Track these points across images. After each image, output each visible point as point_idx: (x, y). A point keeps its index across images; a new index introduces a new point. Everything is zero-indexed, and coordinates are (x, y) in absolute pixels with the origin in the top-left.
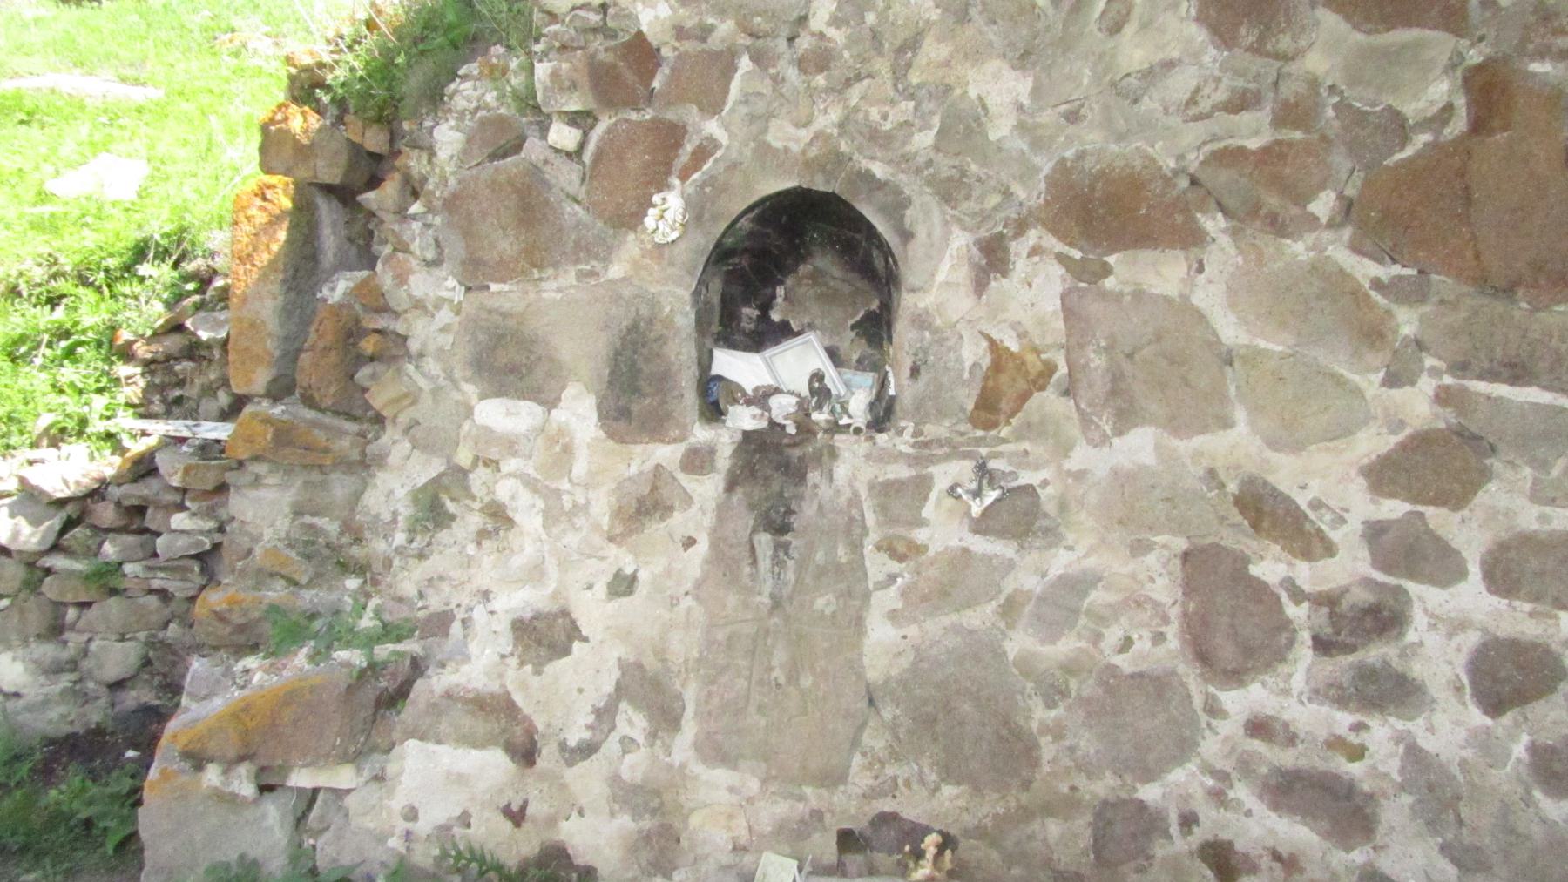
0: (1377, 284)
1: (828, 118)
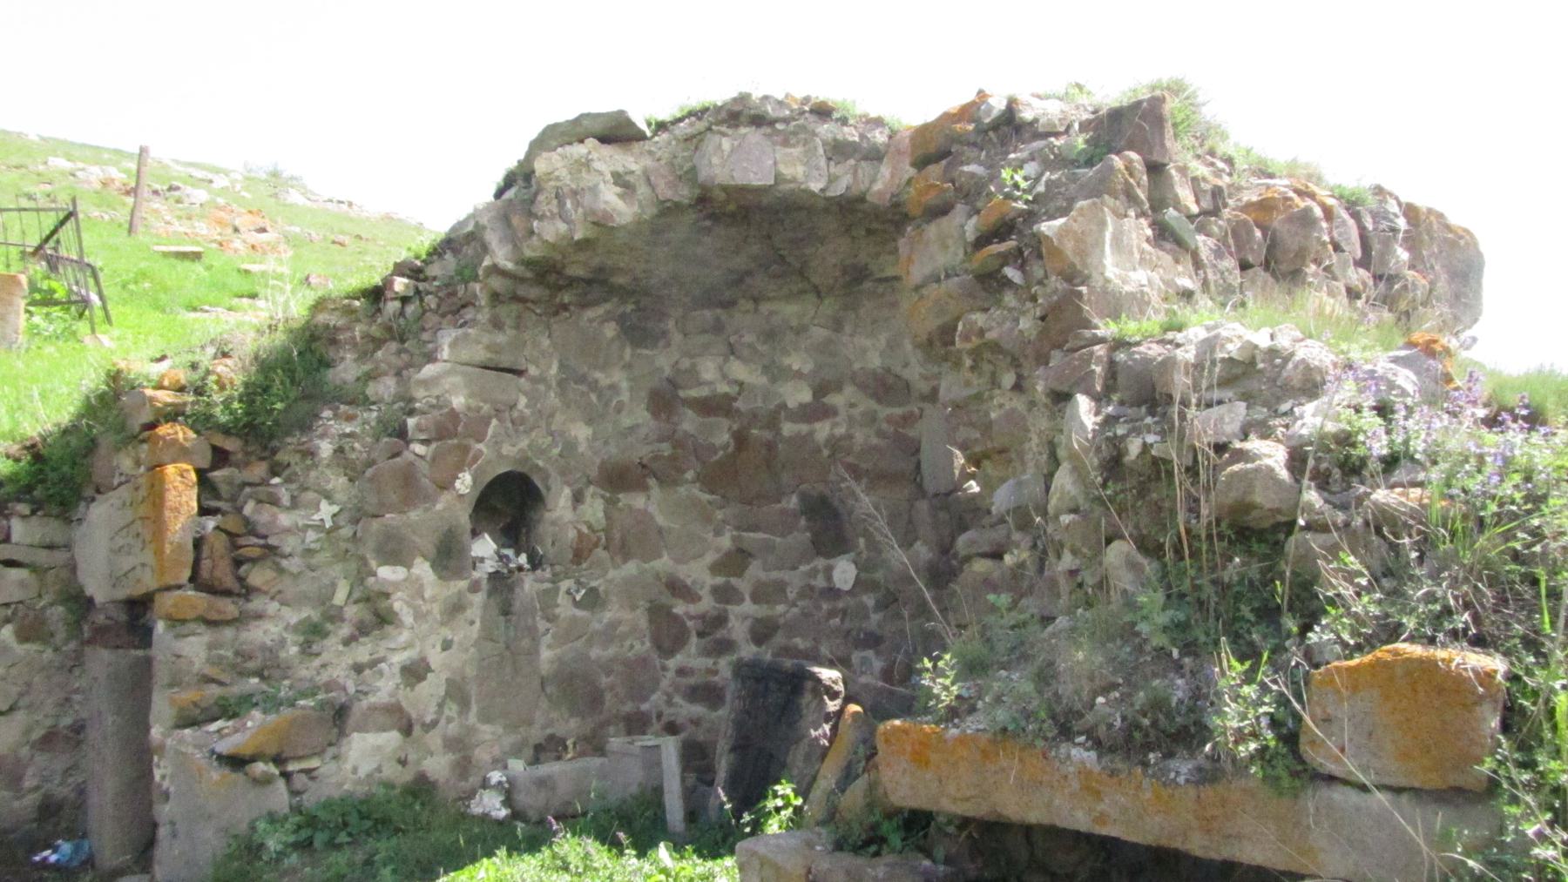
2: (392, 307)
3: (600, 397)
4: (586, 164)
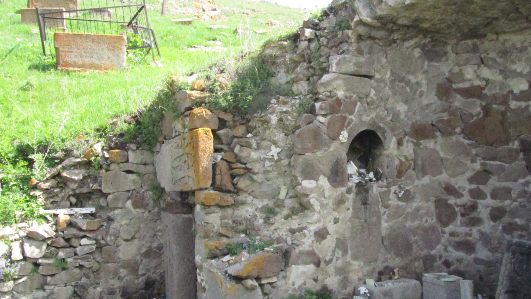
0: (469, 145)
1: (373, 115)
2: (304, 44)
3: (411, 89)
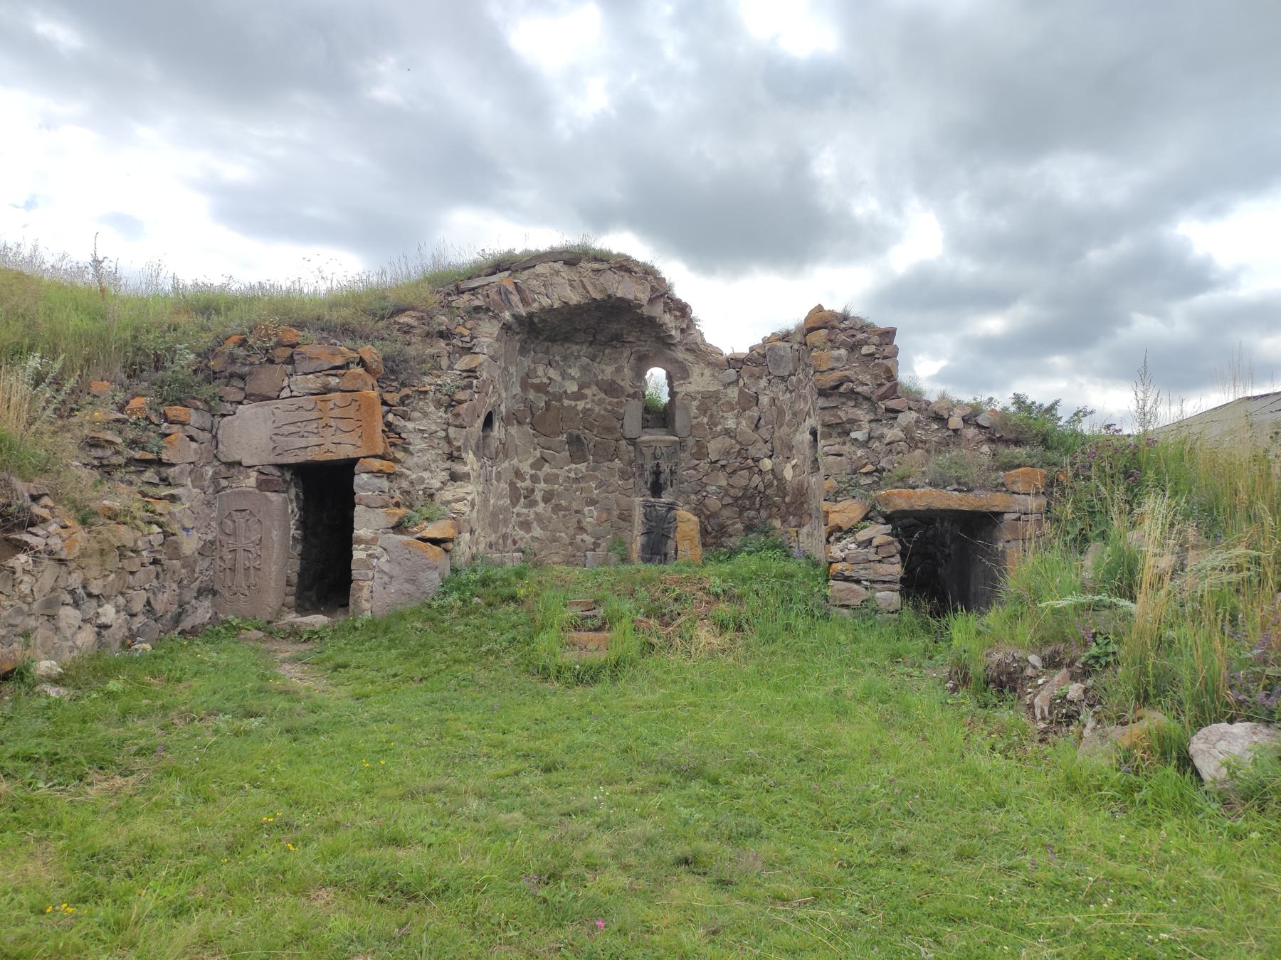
4: (557, 272)
